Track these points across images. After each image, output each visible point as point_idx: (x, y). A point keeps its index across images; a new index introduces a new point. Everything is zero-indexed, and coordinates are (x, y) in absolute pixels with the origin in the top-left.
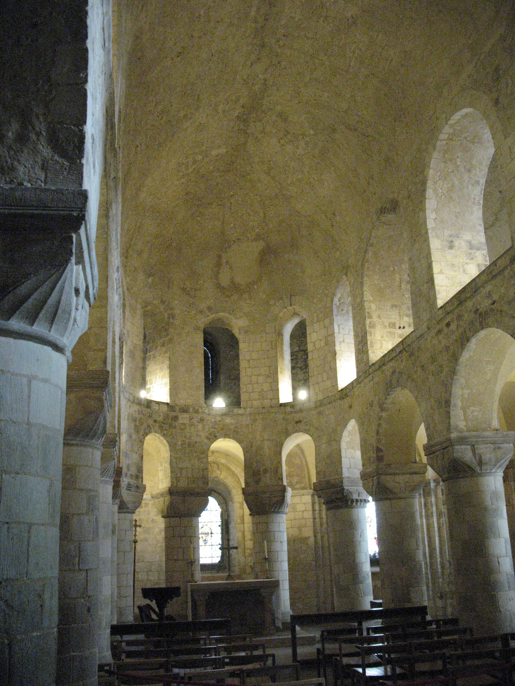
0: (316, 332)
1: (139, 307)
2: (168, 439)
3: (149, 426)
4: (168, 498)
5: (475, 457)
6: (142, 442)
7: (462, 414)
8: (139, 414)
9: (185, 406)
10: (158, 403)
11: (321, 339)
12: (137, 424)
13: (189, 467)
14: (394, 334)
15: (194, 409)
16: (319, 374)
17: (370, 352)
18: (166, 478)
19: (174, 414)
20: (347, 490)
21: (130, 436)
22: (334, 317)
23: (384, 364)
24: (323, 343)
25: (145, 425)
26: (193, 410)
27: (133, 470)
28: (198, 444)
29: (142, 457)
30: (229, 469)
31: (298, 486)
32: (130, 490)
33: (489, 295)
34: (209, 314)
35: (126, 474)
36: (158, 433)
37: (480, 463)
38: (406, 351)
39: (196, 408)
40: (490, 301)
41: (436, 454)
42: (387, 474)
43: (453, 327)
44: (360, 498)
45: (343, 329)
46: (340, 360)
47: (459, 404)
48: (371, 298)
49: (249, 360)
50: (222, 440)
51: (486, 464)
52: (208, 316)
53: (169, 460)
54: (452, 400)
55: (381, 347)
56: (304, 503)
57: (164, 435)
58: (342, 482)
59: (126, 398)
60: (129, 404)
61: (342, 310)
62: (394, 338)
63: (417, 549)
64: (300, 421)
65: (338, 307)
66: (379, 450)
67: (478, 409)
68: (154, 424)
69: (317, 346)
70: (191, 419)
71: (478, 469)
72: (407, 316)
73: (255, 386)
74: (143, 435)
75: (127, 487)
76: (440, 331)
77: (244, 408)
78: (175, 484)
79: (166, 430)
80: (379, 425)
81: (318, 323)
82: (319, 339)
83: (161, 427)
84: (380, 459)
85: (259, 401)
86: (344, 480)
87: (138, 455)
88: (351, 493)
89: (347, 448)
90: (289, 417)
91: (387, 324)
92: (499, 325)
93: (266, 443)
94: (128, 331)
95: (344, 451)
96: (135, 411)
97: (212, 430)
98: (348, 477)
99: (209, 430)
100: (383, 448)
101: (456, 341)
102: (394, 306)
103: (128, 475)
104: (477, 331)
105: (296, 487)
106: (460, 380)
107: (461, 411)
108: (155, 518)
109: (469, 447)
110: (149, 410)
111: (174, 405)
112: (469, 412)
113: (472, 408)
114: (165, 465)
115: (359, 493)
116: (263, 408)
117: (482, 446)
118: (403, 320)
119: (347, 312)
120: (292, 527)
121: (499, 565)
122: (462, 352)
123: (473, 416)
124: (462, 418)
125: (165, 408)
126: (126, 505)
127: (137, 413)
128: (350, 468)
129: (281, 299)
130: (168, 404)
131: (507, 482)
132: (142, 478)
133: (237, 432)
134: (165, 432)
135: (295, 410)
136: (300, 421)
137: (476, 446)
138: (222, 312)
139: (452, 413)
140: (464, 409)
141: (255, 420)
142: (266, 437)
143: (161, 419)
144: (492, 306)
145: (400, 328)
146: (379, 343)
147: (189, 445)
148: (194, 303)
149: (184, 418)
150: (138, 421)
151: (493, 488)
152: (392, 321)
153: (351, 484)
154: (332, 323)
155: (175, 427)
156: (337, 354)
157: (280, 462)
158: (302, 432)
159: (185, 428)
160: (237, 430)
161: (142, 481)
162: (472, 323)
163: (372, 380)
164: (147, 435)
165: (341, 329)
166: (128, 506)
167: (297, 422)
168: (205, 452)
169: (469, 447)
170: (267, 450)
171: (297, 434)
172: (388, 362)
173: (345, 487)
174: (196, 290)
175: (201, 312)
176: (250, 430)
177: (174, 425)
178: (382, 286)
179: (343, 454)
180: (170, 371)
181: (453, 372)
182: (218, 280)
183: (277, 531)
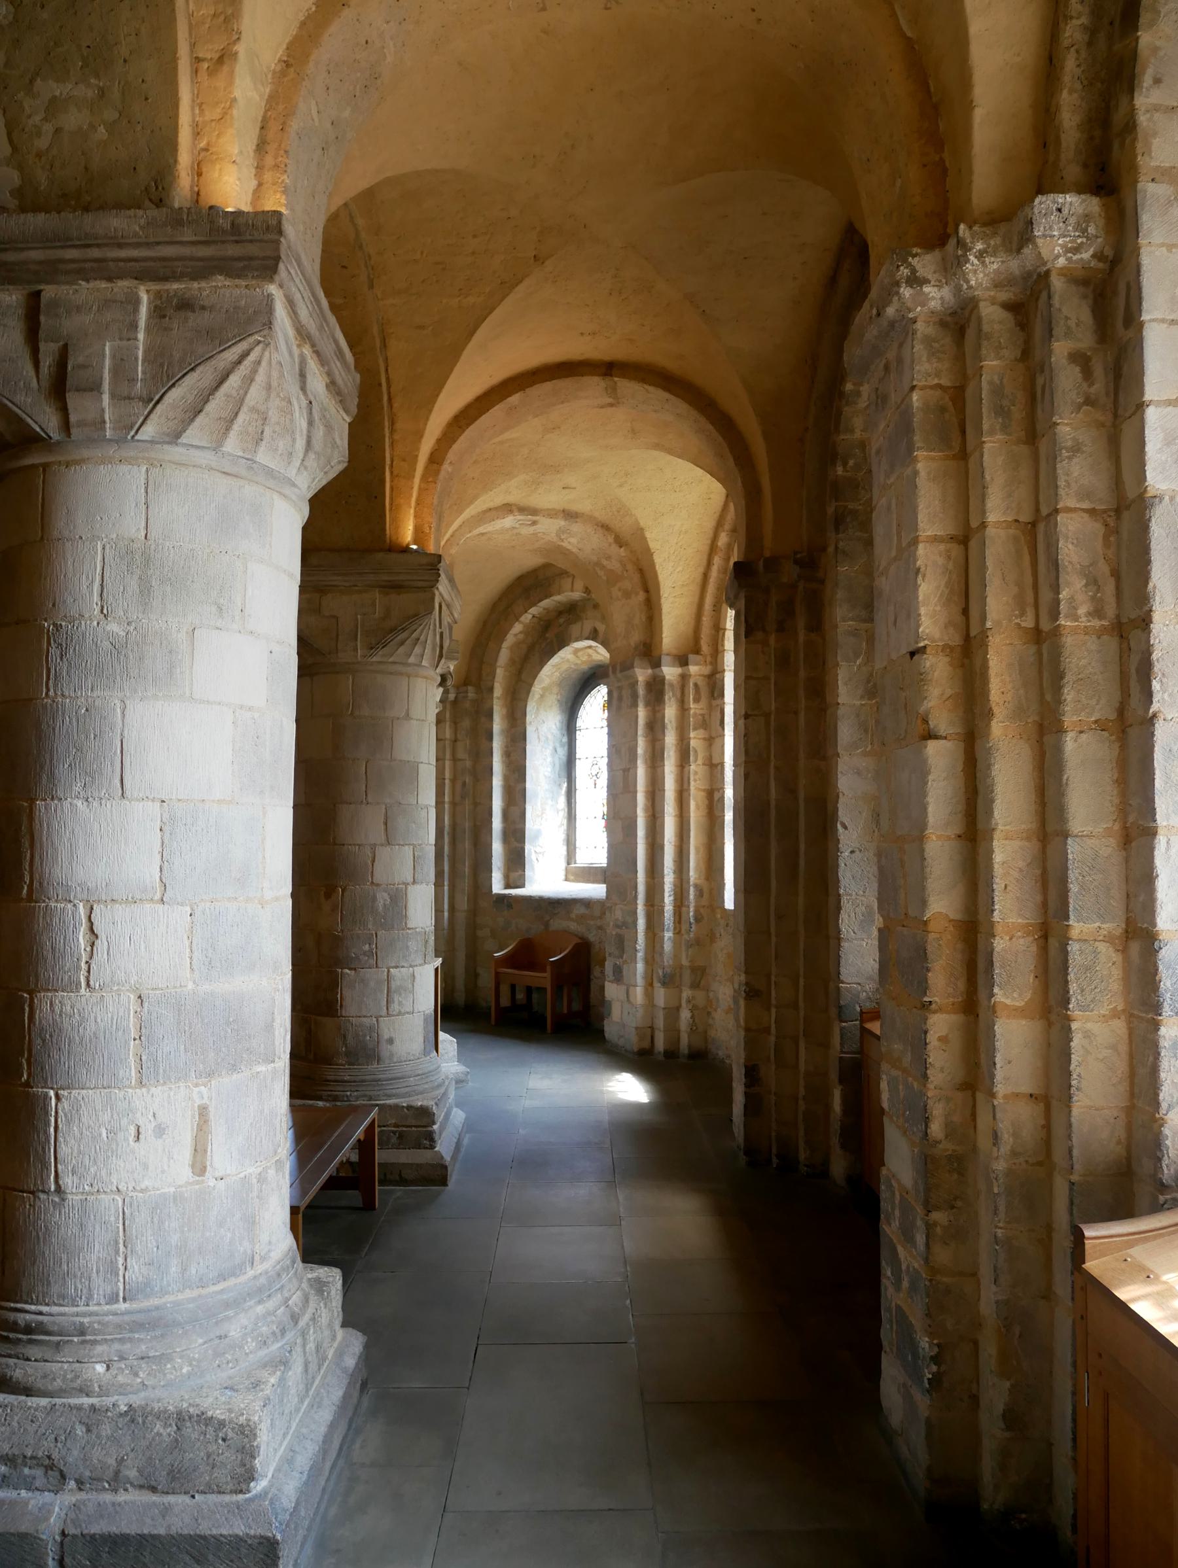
113: (50, 88)
117: (86, 291)
121: (92, 945)
123: (58, 131)
131: (759, 635)
137: (49, 292)
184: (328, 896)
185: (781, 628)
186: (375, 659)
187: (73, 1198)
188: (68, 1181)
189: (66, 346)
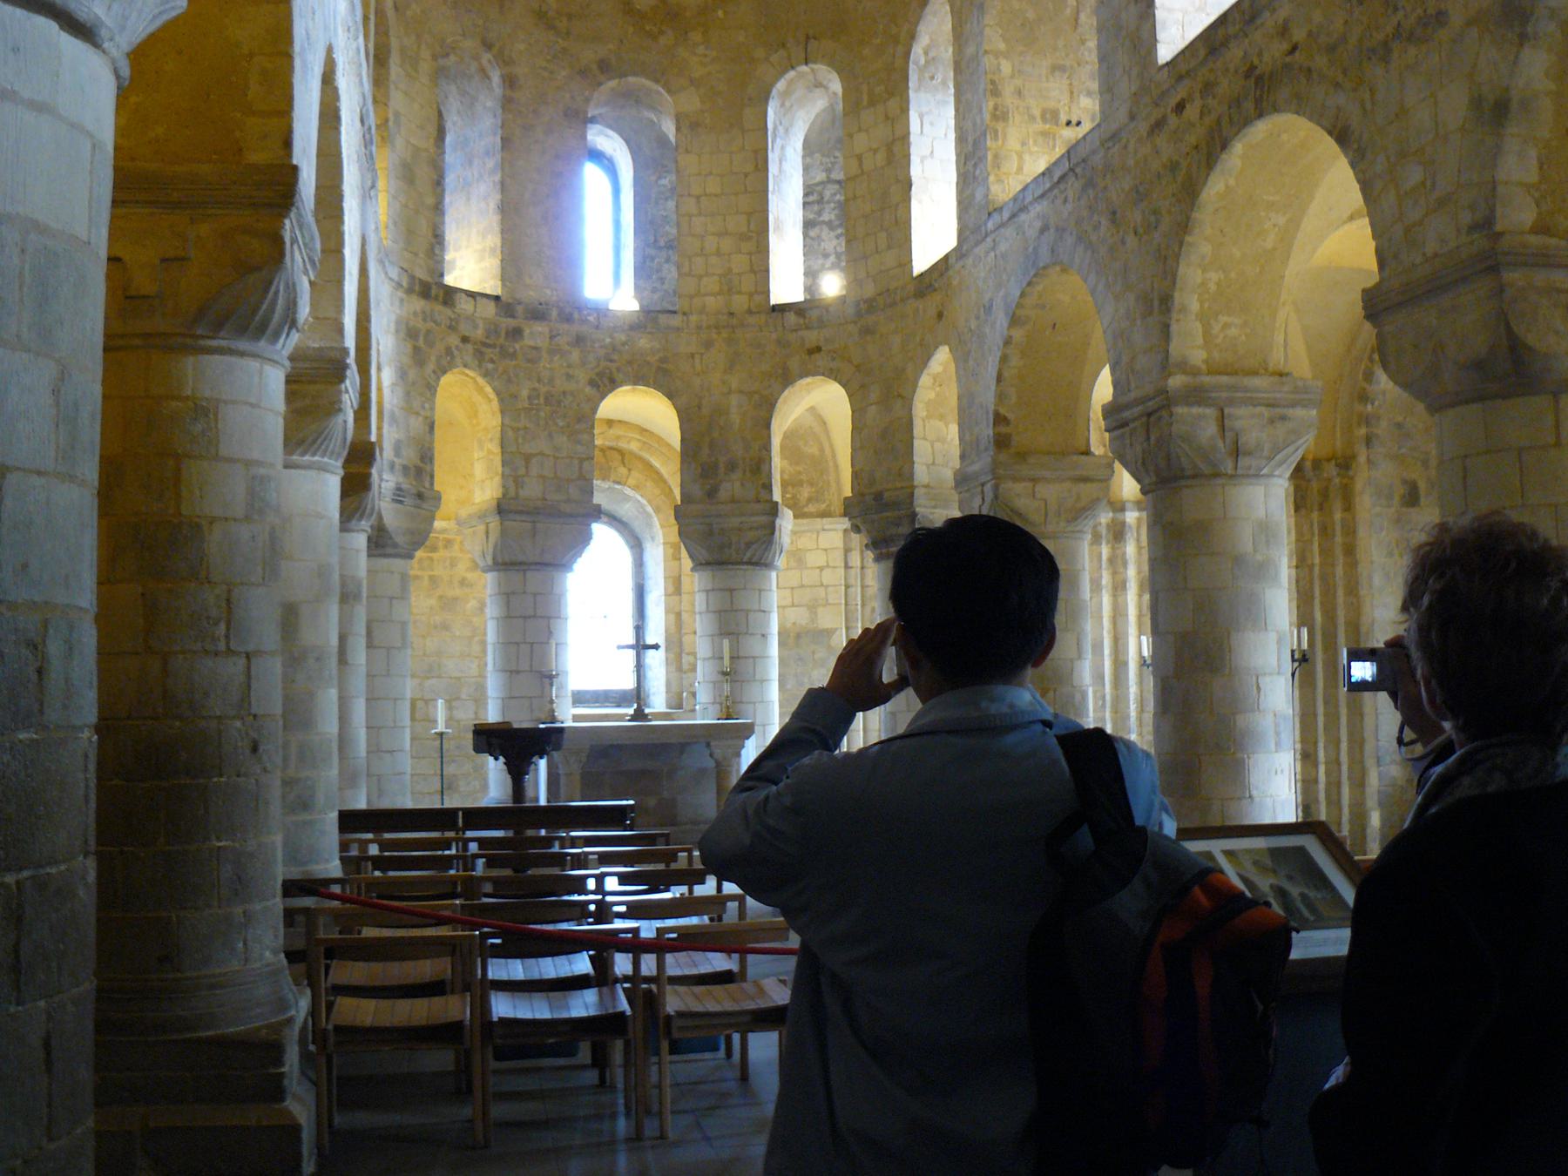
0: (867, 131)
1: (425, 54)
2: (496, 383)
3: (449, 351)
4: (494, 523)
5: (1223, 437)
6: (432, 389)
7: (1200, 330)
8: (424, 320)
9: (541, 304)
10: (472, 295)
11: (878, 148)
12: (421, 343)
13: (548, 452)
14: (1054, 140)
16: (868, 235)
17: (992, 178)
18: (492, 478)
19: (511, 322)
20: (923, 517)
21: (402, 374)
23: (1024, 209)
24: (881, 157)
25: (440, 347)
26: (559, 315)
27: (410, 455)
28: (570, 399)
29: (432, 427)
30: (649, 466)
31: (811, 508)
32: (401, 502)
33: (1284, 31)
36: (474, 370)
37: (1236, 452)
38: (1076, 175)
40: (1286, 46)
41: (1132, 425)
42: (1015, 479)
43: (1191, 112)
46: (920, 202)
47: (1195, 306)
48: (1002, 46)
49: (698, 198)
50: (628, 391)
51: (1249, 453)
52: (600, 84)
53: (498, 435)
54: (1177, 295)
55: (1020, 169)
56: (826, 550)
57: (486, 374)
58: (912, 495)
59: (391, 279)
60: (400, 294)
61: (932, 78)
62: (1054, 146)
63: (1080, 656)
64: (819, 349)
65: (922, 70)
66: (999, 419)
67: (1237, 321)
68: (461, 345)
69: (868, 164)
70: (552, 337)
71: (1228, 466)
72: (1089, 94)
73: (714, 260)
74: (434, 372)
75: (394, 494)
76: (1159, 125)
77: (684, 314)
78: (512, 493)
79: (492, 361)
80: (1004, 359)
82: (871, 149)
83: (479, 355)
84: (1001, 442)
86: (916, 491)
87: (421, 419)
89: (929, 417)
91: (1037, 112)
92: (1300, 105)
93: (734, 400)
94: (397, 114)
95: (921, 423)
96: (415, 314)
97: (603, 364)
98: (927, 486)
99: (598, 365)
100: (1010, 416)
101: (1196, 147)
102: (1057, 68)
103: (397, 467)
104: (1247, 122)
105: (806, 510)
106: (1201, 246)
107: (1198, 325)
108: (469, 575)
109: (1210, 412)
110: (448, 312)
111: (510, 301)
112: (1216, 329)
113: (1224, 319)
116: (731, 314)
118: (1078, 103)
119: (944, 83)
120: (793, 605)
122: (1208, 175)
123: (1224, 337)
124: (1200, 341)
125: (490, 309)
126: (391, 538)
127: (420, 319)
128: (933, 463)
129: (784, 45)
130: (497, 298)
131: (1303, 512)
132: (432, 477)
134: (490, 366)
135: (807, 321)
136: (819, 349)
137: (1226, 411)
139: (1174, 328)
140: (1205, 319)
141: (708, 344)
142: (734, 386)
143: (479, 333)
144: (1288, 59)
145: (1069, 123)
146: (1015, 157)
147: (547, 401)
148: (564, 50)
149: (535, 333)
151: (1262, 513)
152: (1052, 104)
153: (933, 503)
154: (905, 110)
155: (513, 356)
156: (913, 188)
157: (767, 447)
158: (823, 375)
160: (664, 366)
161: (432, 484)
162: (1236, 102)
163: (993, 249)
164: (445, 372)
168: (585, 419)
169: (1210, 412)
170: (735, 418)
171: (809, 380)
172: (1031, 203)
173: (917, 509)
174: (570, 17)
175: (583, 73)
176: (698, 367)
177: (511, 350)
178: (1031, 15)
180: (502, 219)
181: (1184, 226)
183: (755, 611)
185: (1321, 508)
186: (1070, 529)
187: (1257, 800)
188: (1254, 793)
189: (1237, 435)
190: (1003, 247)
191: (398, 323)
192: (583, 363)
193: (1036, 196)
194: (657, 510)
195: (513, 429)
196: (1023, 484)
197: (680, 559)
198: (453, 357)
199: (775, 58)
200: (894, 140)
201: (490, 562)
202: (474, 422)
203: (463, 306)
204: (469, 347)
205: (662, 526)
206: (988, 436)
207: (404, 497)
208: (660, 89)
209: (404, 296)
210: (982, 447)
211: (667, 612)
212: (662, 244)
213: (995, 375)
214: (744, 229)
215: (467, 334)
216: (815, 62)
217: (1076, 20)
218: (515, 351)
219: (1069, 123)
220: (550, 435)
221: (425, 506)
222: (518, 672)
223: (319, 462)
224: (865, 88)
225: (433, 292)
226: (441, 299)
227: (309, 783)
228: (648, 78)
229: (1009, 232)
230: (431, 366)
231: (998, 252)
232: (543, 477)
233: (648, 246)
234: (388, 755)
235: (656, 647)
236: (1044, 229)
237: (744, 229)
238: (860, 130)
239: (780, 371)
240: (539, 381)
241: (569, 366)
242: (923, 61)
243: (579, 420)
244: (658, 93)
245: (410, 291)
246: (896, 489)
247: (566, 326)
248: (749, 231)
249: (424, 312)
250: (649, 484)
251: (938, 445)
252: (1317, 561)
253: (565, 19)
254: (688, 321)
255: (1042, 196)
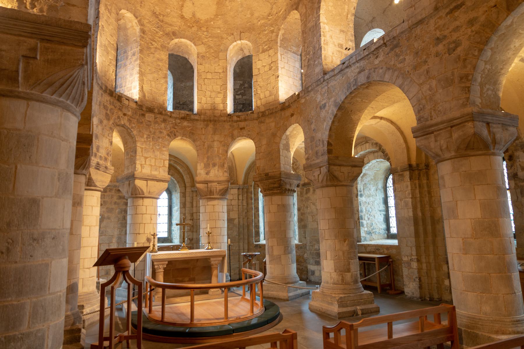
1: (114, 11)
3: (119, 117)
8: (110, 104)
12: (108, 112)
15: (159, 110)
20: (283, 181)
21: (101, 122)
22: (279, 48)
24: (267, 68)
28: (161, 140)
30: (176, 169)
32: (99, 169)
34: (173, 37)
35: (96, 155)
39: (161, 110)
42: (334, 165)
44: (290, 188)
45: (284, 58)
47: (479, 80)
52: (173, 39)
64: (244, 128)
66: (329, 144)
68: (123, 116)
73: (209, 99)
74: (113, 123)
75: (96, 166)
79: (134, 124)
80: (333, 122)
81: (264, 53)
85: (211, 111)
87: (107, 139)
88: (286, 183)
90: (235, 124)
91: (337, 45)
96: (107, 101)
103: (97, 155)
110: (119, 104)
114: (131, 154)
115: (290, 185)
116: (215, 116)
125: (134, 105)
126: (94, 183)
129: (233, 34)
130: (136, 102)
133: (193, 134)
134: (133, 125)
136: (244, 128)
138: (184, 38)
140: (482, 85)
141: (207, 126)
143: (130, 113)
146: (330, 57)
150: (109, 110)
152: (341, 42)
153: (286, 177)
154: (276, 53)
155: (142, 123)
159: (151, 125)
165: (282, 58)
166: (97, 184)
167: (241, 129)
171: (240, 138)
172: (353, 64)
174: (164, 16)
175: (167, 34)
179: (281, 154)
182: (182, 12)
184: (345, 242)
185: (419, 179)
190: (332, 83)
191: (100, 102)
192: (165, 128)
193: (358, 59)
194: (178, 182)
195: (141, 148)
196: (337, 167)
197: (185, 197)
198: (120, 120)
199: (230, 38)
200: (272, 63)
201: (130, 195)
202: (126, 146)
203: (124, 102)
204: (126, 118)
205: (180, 187)
206: (324, 150)
207: (100, 167)
208: (193, 45)
209: (103, 93)
210: (320, 154)
211: (180, 213)
212: (181, 103)
213: (328, 128)
214: (219, 90)
215: (125, 113)
216: (242, 40)
217: (347, 16)
218: (142, 122)
219: (346, 49)
220: (154, 151)
221: (108, 172)
222: (139, 234)
223: (63, 102)
224: (261, 47)
225: (114, 95)
226: (117, 98)
227: (39, 335)
228: (188, 40)
229: (339, 76)
230: (111, 122)
231: (329, 86)
232: (151, 165)
233: (177, 103)
234: (88, 270)
235: (177, 225)
236: (360, 72)
237: (219, 90)
238: (259, 60)
239: (231, 135)
240: (150, 132)
241: (161, 129)
242: (281, 39)
243: (164, 147)
244: (191, 46)
245: (105, 91)
246: (273, 172)
247: (160, 116)
248: (221, 90)
249: (110, 101)
250: (176, 174)
251: (286, 158)
252: (418, 196)
253: (162, 16)
254: (201, 117)
255: (361, 59)
